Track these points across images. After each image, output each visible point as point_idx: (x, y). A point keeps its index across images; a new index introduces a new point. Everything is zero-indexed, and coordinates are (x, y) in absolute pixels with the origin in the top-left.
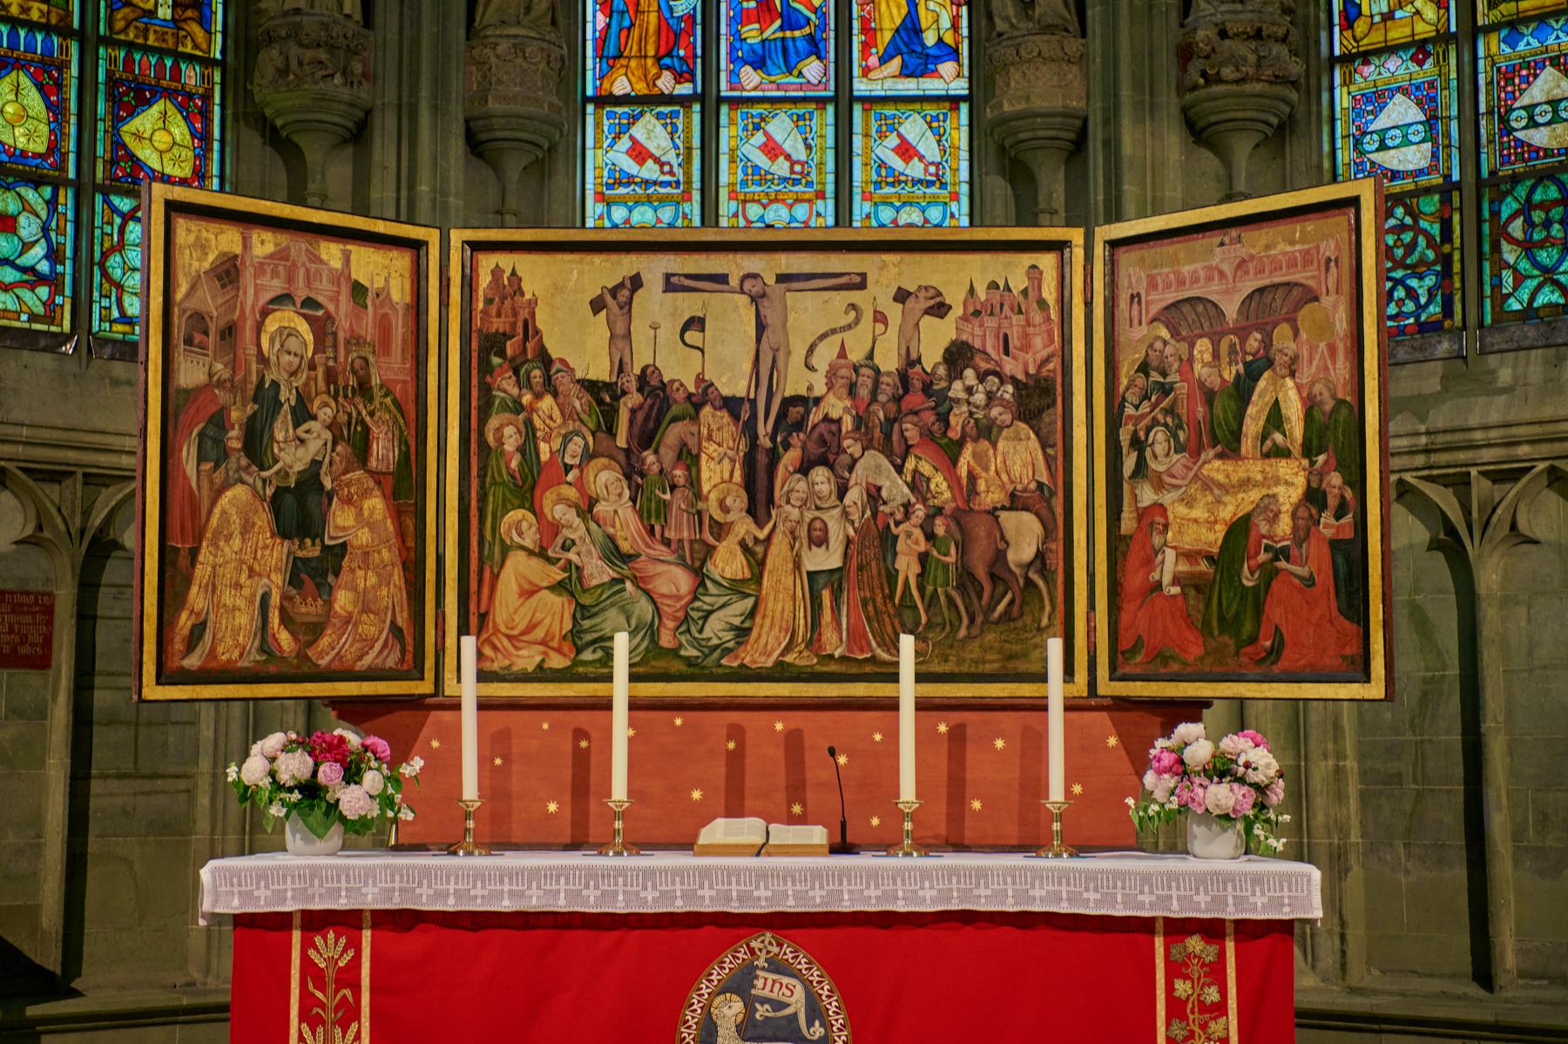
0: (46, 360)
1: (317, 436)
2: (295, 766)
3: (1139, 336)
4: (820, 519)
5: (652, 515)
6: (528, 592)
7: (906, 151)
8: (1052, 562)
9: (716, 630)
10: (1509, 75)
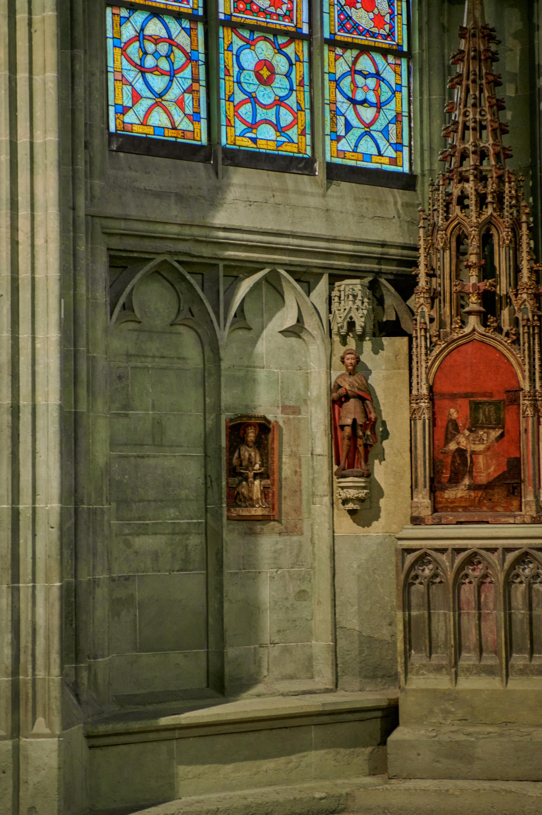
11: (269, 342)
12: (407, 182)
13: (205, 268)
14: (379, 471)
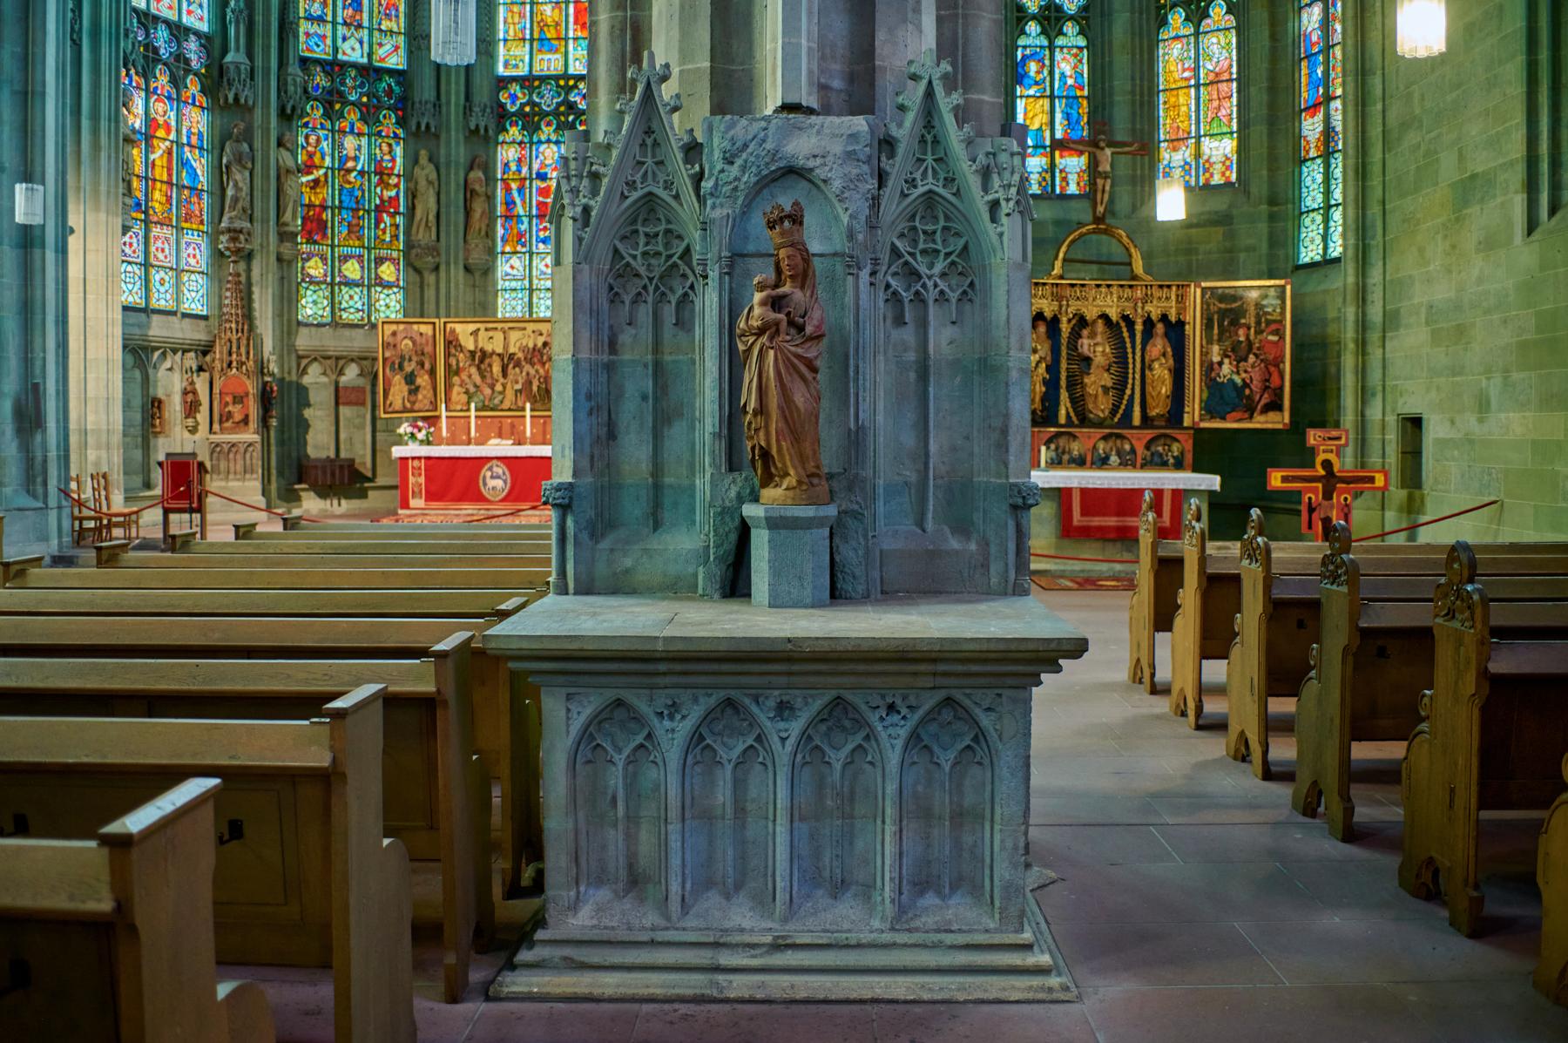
1: (413, 364)
2: (409, 430)
4: (517, 377)
5: (483, 377)
9: (496, 401)
11: (162, 372)
12: (205, 318)
13: (144, 349)
14: (198, 416)
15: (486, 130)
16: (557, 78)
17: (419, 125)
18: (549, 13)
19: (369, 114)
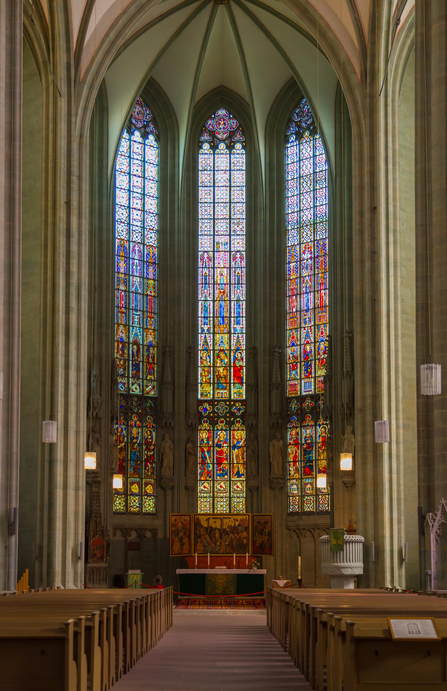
0: (139, 516)
3: (255, 523)
5: (211, 539)
6: (200, 546)
7: (238, 487)
8: (248, 543)
9: (217, 549)
10: (305, 484)
15: (195, 425)
16: (225, 401)
17: (166, 423)
18: (221, 371)
19: (141, 418)
